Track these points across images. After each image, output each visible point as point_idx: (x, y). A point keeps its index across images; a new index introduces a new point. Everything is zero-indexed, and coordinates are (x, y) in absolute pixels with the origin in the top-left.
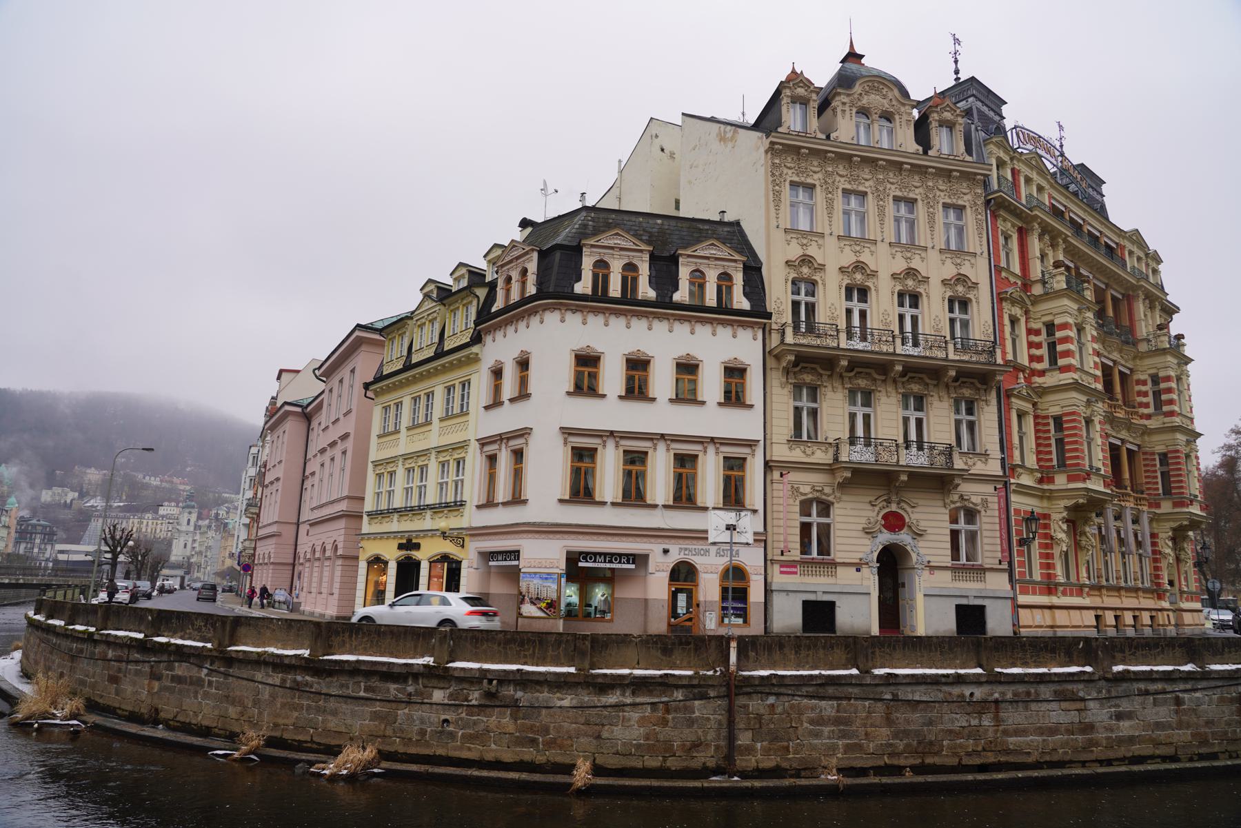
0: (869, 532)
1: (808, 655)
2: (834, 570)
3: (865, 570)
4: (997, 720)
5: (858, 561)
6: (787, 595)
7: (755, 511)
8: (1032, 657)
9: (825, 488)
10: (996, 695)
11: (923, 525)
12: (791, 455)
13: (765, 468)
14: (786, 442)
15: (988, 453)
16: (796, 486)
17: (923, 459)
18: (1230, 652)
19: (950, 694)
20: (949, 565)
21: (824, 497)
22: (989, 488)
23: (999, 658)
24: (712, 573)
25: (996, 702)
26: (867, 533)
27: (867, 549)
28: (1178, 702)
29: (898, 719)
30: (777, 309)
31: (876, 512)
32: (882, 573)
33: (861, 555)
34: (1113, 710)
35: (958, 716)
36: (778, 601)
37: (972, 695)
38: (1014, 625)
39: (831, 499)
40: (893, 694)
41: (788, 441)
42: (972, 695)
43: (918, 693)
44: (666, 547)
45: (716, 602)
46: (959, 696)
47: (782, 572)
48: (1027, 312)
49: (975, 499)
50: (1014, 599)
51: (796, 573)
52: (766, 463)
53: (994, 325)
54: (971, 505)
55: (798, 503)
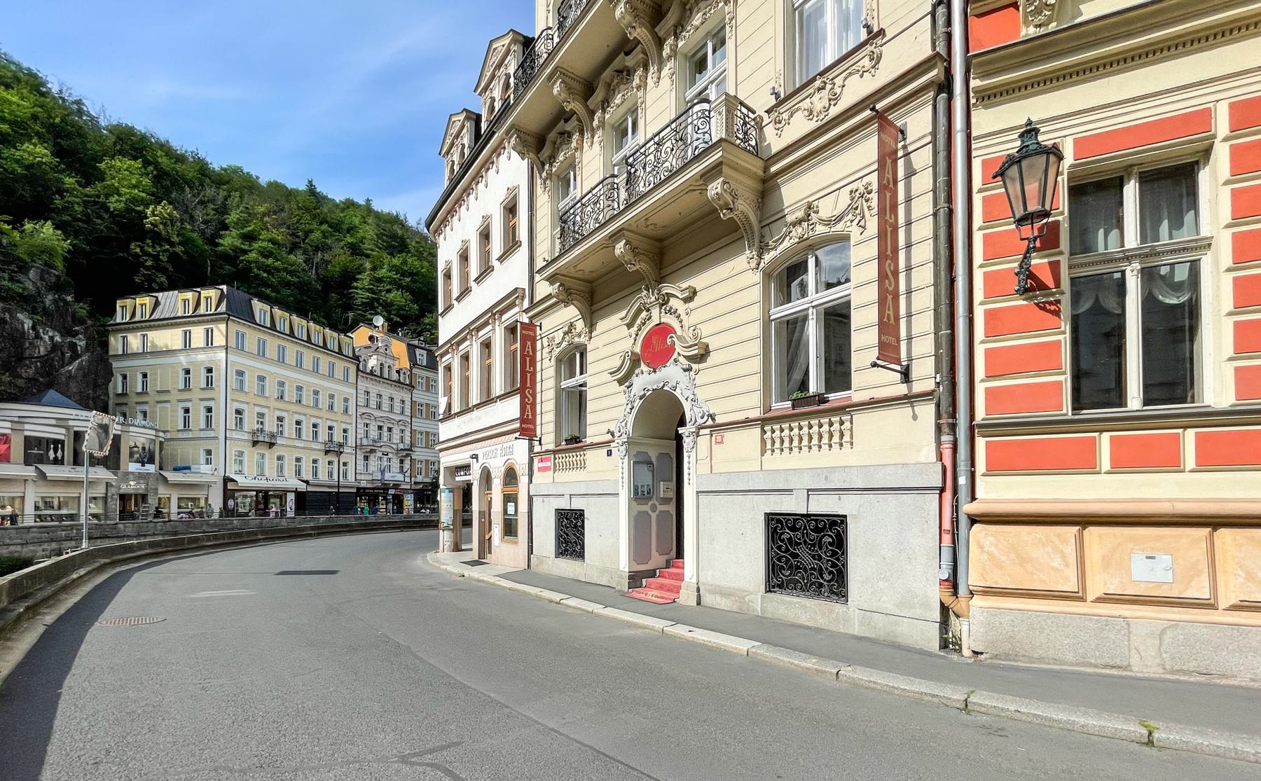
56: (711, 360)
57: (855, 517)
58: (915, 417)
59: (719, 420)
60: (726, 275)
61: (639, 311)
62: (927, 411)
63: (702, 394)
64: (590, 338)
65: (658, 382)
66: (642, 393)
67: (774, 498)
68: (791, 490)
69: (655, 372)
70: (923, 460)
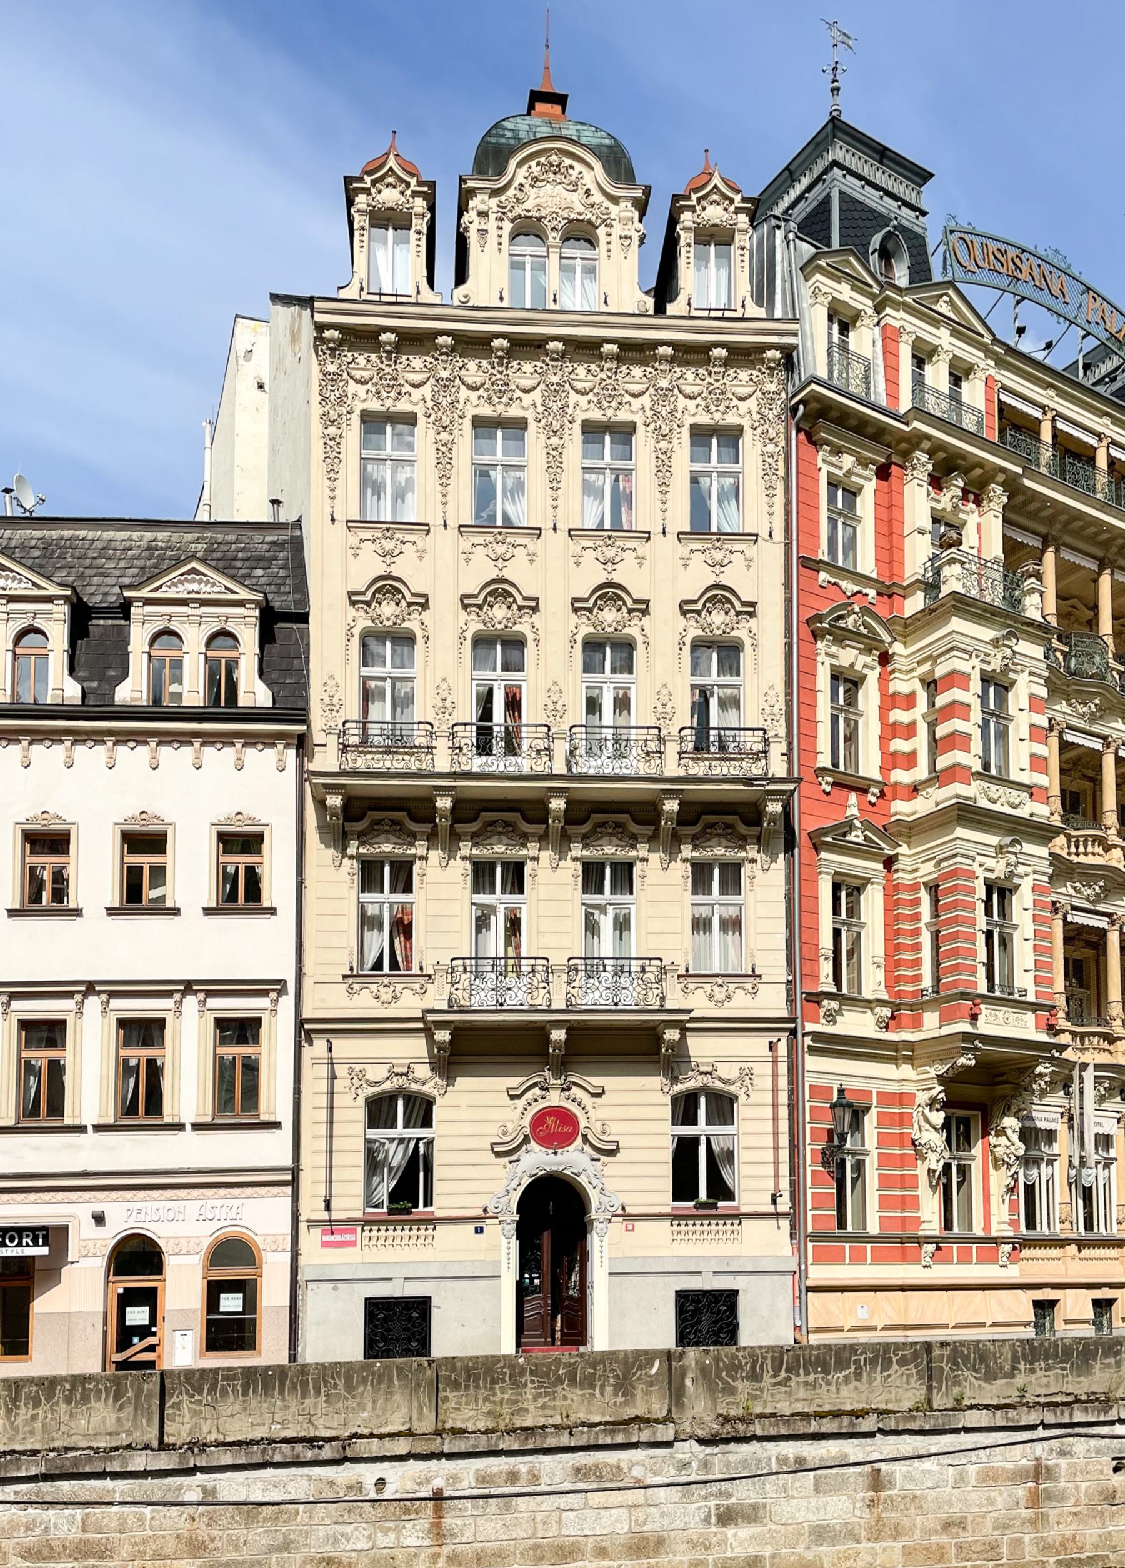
0: (505, 1152)
1: (34, 1417)
3: (490, 1227)
4: (438, 1532)
7: (276, 1125)
8: (535, 1400)
9: (417, 1067)
10: (438, 1483)
13: (298, 1034)
15: (757, 973)
17: (597, 994)
18: (1033, 1371)
19: (331, 1483)
21: (414, 1087)
22: (757, 1045)
24: (188, 1253)
25: (438, 1497)
28: (877, 1482)
29: (213, 1540)
31: (521, 1109)
32: (526, 1233)
34: (712, 1503)
35: (348, 1529)
36: (313, 1301)
37: (381, 1483)
38: (797, 1328)
39: (428, 1089)
40: (205, 1490)
42: (381, 1483)
43: (260, 1485)
44: (98, 1207)
45: (195, 1310)
46: (350, 1488)
48: (885, 659)
49: (727, 1071)
50: (799, 1273)
52: (300, 1023)
53: (789, 693)
54: (718, 1084)
57: (745, 1291)
58: (779, 1228)
59: (629, 1210)
60: (637, 1088)
61: (535, 1085)
62: (785, 1223)
63: (611, 1185)
65: (560, 1164)
66: (534, 1172)
67: (683, 1278)
69: (556, 1153)
70: (786, 1254)
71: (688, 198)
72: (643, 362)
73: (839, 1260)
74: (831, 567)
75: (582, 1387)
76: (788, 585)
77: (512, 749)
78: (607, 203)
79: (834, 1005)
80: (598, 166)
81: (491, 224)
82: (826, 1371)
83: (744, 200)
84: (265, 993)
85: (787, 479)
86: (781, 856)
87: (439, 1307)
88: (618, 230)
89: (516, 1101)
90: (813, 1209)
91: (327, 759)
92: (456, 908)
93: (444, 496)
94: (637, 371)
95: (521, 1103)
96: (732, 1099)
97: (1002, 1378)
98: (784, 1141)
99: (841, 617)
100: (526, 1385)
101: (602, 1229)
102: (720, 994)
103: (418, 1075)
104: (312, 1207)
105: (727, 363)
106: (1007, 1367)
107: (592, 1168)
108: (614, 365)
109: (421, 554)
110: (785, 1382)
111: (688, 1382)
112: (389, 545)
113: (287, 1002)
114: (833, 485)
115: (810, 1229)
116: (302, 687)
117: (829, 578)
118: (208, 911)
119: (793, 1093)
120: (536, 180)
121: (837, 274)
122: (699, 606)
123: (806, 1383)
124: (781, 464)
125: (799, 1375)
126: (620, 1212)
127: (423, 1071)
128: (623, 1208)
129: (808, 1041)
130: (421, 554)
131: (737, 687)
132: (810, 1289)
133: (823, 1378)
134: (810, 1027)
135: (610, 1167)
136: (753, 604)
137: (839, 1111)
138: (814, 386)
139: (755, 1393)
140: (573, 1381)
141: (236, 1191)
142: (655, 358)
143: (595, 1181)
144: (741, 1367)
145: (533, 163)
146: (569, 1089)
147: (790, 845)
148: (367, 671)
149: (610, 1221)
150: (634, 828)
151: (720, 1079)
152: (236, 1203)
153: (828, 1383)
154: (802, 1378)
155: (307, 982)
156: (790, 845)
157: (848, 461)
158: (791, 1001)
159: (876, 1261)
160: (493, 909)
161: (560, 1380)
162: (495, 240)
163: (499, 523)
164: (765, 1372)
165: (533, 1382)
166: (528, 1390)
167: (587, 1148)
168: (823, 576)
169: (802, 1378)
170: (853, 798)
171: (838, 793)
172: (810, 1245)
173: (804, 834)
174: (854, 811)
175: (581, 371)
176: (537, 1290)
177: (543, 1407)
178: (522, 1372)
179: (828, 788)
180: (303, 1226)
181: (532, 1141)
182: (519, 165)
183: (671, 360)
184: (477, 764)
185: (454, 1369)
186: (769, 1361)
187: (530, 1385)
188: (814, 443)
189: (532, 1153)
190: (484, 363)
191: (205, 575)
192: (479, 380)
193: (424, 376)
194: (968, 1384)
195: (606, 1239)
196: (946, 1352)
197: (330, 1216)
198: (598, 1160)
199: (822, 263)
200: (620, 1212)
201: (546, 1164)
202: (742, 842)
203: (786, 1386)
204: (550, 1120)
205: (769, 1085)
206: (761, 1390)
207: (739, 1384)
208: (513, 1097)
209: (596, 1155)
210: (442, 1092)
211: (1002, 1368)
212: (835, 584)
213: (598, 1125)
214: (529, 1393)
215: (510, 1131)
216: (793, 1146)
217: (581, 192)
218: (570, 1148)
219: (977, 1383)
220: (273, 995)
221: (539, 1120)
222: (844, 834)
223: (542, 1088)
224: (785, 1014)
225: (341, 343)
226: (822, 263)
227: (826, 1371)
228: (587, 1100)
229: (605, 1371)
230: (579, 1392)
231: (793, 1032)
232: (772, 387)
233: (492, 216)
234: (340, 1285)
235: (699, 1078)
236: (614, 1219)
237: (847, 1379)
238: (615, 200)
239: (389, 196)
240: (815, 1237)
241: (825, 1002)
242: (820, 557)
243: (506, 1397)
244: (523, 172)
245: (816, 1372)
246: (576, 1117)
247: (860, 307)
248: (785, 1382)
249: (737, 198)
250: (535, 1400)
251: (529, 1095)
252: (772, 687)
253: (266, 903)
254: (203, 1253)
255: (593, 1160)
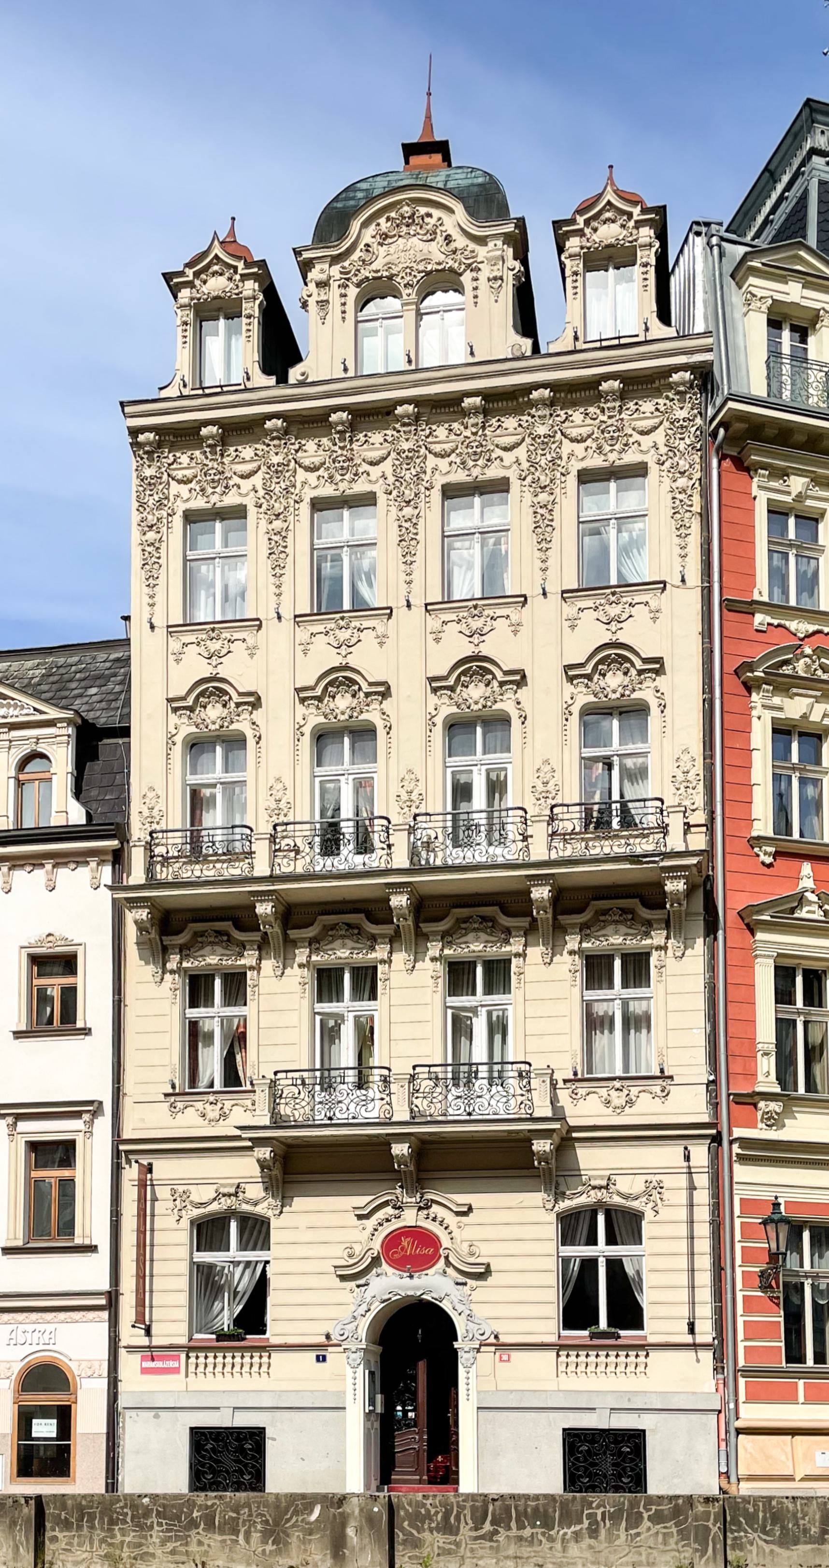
2: (265, 1359)
5: (322, 1339)
6: (156, 1416)
8: (163, 1543)
11: (486, 1253)
12: (174, 1123)
14: (162, 1098)
16: (181, 1189)
20: (553, 1339)
23: (69, 1544)
26: (343, 1278)
27: (345, 1313)
30: (146, 813)
33: (328, 1327)
41: (167, 1095)
47: (145, 1371)
49: (624, 1184)
51: (176, 1371)
54: (617, 1200)
55: (185, 1223)
56: (490, 1280)
58: (698, 1361)
59: (503, 1339)
61: (386, 1204)
62: (707, 1357)
63: (479, 1311)
64: (281, 1212)
65: (418, 1289)
68: (594, 1409)
69: (411, 1277)
70: (707, 1390)
71: (572, 221)
72: (518, 411)
73: (790, 1398)
74: (768, 607)
75: (222, 1532)
76: (707, 633)
77: (364, 846)
78: (472, 246)
79: (775, 1106)
80: (459, 208)
81: (334, 293)
82: (548, 1524)
83: (644, 211)
84: (77, 1115)
85: (705, 516)
86: (700, 941)
87: (274, 1439)
88: (486, 272)
89: (364, 1221)
90: (746, 1339)
91: (137, 875)
92: (292, 1018)
93: (279, 587)
94: (510, 422)
95: (371, 1223)
96: (636, 1218)
97: (806, 1543)
98: (704, 1262)
99: (786, 662)
100: (151, 1528)
101: (467, 1360)
102: (618, 1099)
103: (249, 1195)
104: (130, 1335)
105: (623, 396)
106: (814, 1530)
107: (458, 1293)
108: (480, 419)
109: (252, 652)
110: (490, 1536)
111: (350, 1532)
112: (214, 646)
113: (104, 1124)
114: (777, 512)
115: (741, 1362)
116: (123, 801)
117: (769, 619)
118: (18, 1035)
119: (716, 1208)
120: (385, 236)
121: (781, 274)
122: (588, 669)
123: (520, 1539)
124: (696, 499)
125: (510, 1529)
126: (492, 1340)
127: (255, 1191)
128: (496, 1337)
129: (736, 1148)
130: (252, 652)
131: (645, 754)
132: (739, 1431)
133: (543, 1534)
134: (738, 1132)
135: (481, 1291)
136: (659, 660)
137: (771, 1228)
138: (731, 405)
139: (448, 1546)
140: (210, 1525)
141: (49, 1316)
142: (532, 404)
143: (460, 1308)
144: (429, 1516)
145: (382, 221)
146: (428, 1207)
147: (711, 928)
148: (193, 780)
149: (478, 1351)
150: (505, 921)
151: (619, 1194)
152: (50, 1327)
153: (551, 1539)
154: (514, 1532)
155: (127, 1104)
156: (711, 928)
157: (797, 484)
158: (715, 1105)
159: (810, 1399)
160: (339, 1018)
161: (194, 1524)
162: (338, 309)
163: (347, 605)
164: (462, 1525)
165: (160, 1524)
166: (154, 1533)
167: (450, 1271)
168: (759, 618)
169: (514, 1532)
170: (807, 868)
171: (781, 863)
172: (742, 1381)
173: (732, 916)
174: (809, 883)
175: (441, 432)
176: (407, 1423)
177: (173, 1552)
178: (147, 1513)
179: (768, 860)
180: (122, 1352)
181: (385, 1266)
182: (365, 224)
183: (551, 403)
184: (323, 864)
185: (64, 1507)
186: (467, 1512)
187: (156, 1528)
188: (747, 470)
189: (384, 1277)
190: (325, 441)
191: (13, 699)
192: (317, 460)
193: (254, 465)
194: (754, 1549)
195: (473, 1370)
196: (714, 1509)
197: (151, 1341)
198: (465, 1284)
199: (756, 264)
200: (492, 1340)
201: (400, 1288)
202: (647, 927)
203: (491, 1540)
204: (405, 1242)
205: (682, 1197)
206: (458, 1544)
207: (426, 1535)
208: (360, 1217)
209: (461, 1279)
210: (277, 1212)
211: (806, 1531)
212: (779, 626)
213: (465, 1247)
214: (156, 1536)
215: (357, 1253)
216: (718, 1269)
217: (440, 239)
218: (431, 1271)
219: (767, 1548)
220: (86, 1117)
221: (392, 1241)
222: (792, 910)
223: (394, 1207)
224: (705, 1119)
225: (160, 445)
226: (756, 264)
227: (548, 1524)
228: (451, 1219)
229: (250, 1515)
230: (219, 1538)
231: (717, 1139)
232: (682, 414)
233: (334, 285)
234: (162, 1414)
235: (592, 1193)
236: (483, 1349)
237: (577, 1536)
238: (482, 241)
239: (216, 285)
240: (747, 1372)
241: (762, 1104)
242: (756, 597)
243: (128, 1539)
244: (371, 230)
245: (534, 1526)
246: (437, 1237)
247: (818, 305)
248: (490, 1536)
249: (636, 211)
250: (163, 1543)
251: (380, 1215)
252: (686, 751)
253: (80, 1024)
254: (14, 1377)
255: (457, 1284)
